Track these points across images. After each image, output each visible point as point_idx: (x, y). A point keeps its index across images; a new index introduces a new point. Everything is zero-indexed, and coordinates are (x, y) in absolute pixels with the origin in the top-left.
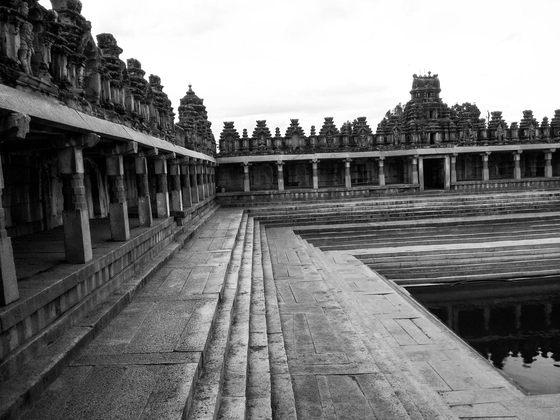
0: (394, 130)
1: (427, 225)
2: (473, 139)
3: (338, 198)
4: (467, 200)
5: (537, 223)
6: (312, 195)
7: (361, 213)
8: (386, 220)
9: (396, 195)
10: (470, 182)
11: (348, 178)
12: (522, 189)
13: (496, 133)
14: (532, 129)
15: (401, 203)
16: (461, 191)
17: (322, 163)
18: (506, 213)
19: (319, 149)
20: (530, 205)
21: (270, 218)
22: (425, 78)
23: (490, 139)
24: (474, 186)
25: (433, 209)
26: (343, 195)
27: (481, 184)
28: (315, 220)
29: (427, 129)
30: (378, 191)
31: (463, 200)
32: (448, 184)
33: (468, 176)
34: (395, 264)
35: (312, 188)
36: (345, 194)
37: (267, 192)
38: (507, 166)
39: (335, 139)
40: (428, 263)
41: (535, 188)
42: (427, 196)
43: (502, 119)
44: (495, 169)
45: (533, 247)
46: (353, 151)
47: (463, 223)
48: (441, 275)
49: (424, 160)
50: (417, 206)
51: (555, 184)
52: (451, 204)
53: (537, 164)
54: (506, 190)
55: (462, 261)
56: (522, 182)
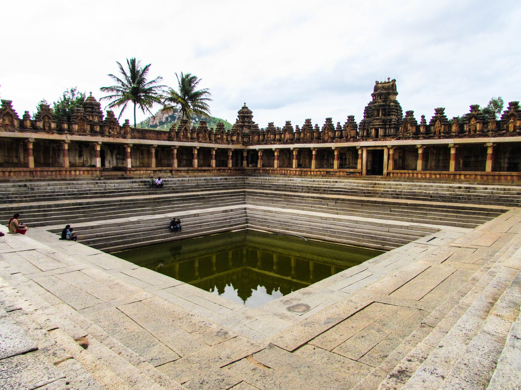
0: (348, 126)
1: (318, 198)
2: (409, 133)
3: (306, 175)
4: (379, 184)
5: (399, 208)
6: (292, 172)
7: (299, 186)
8: (308, 192)
9: (344, 177)
10: (403, 171)
11: (313, 162)
12: (454, 180)
13: (432, 128)
14: (472, 123)
15: (330, 182)
16: (394, 177)
17: (300, 150)
18: (398, 198)
19: (298, 141)
20: (429, 194)
21: (252, 184)
22: (385, 83)
23: (426, 134)
24: (407, 175)
25: (345, 189)
26: (309, 174)
27: (413, 174)
28: (271, 187)
29: (372, 125)
30: (331, 173)
31: (375, 184)
32: (385, 171)
33: (431, 167)
34: (259, 216)
35: (292, 167)
36: (311, 173)
37: (268, 168)
38: (473, 159)
39: (308, 134)
40: (277, 219)
41: (467, 181)
42: (364, 180)
43: (444, 115)
44: (460, 161)
45: (357, 222)
46: (318, 143)
47: (343, 200)
48: (276, 227)
49: (368, 152)
50: (337, 185)
51: (494, 179)
52: (362, 186)
53: (509, 159)
54: (435, 181)
55: (297, 222)
56: (455, 175)
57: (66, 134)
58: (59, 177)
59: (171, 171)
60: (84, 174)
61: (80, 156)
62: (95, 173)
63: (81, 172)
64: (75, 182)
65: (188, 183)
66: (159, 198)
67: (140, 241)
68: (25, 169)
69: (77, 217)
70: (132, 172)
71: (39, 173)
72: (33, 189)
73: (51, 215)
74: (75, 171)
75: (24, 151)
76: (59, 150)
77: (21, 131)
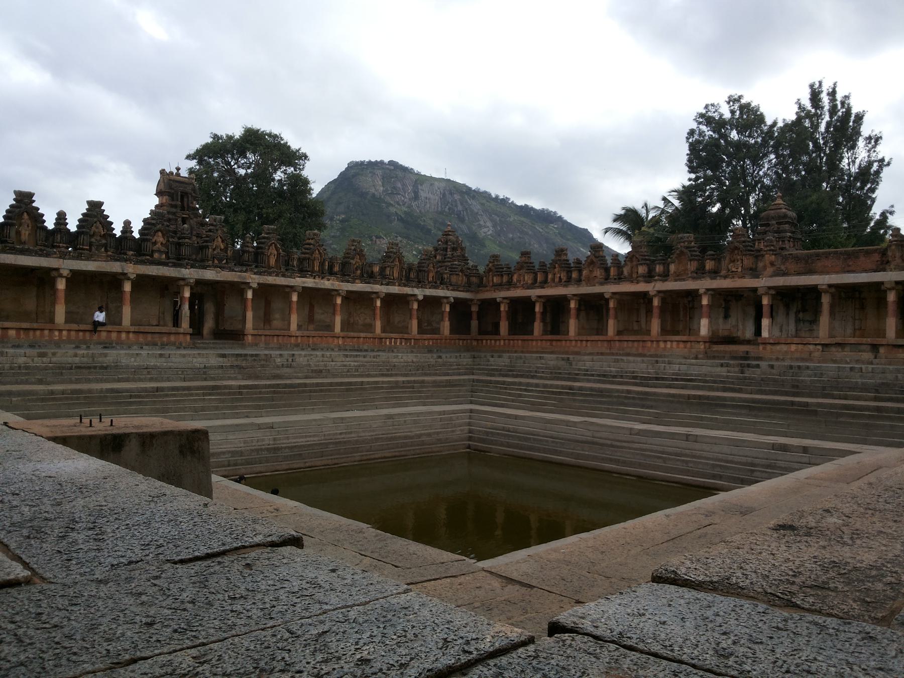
57: (656, 280)
58: (640, 351)
59: (875, 348)
60: (678, 347)
61: (726, 316)
62: (697, 346)
63: (675, 344)
64: (624, 358)
65: (861, 376)
66: (700, 397)
67: (539, 450)
68: (601, 338)
69: (545, 404)
70: (769, 347)
71: (617, 344)
72: (571, 364)
73: (526, 396)
74: (665, 341)
75: (647, 312)
76: (693, 308)
77: (602, 284)
